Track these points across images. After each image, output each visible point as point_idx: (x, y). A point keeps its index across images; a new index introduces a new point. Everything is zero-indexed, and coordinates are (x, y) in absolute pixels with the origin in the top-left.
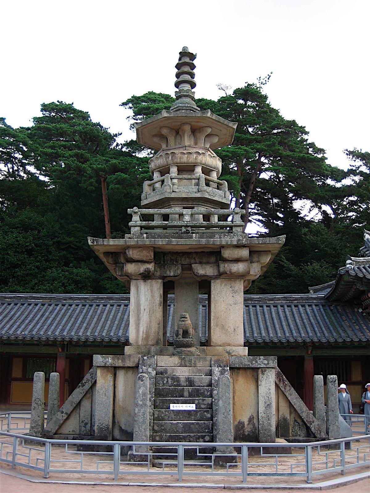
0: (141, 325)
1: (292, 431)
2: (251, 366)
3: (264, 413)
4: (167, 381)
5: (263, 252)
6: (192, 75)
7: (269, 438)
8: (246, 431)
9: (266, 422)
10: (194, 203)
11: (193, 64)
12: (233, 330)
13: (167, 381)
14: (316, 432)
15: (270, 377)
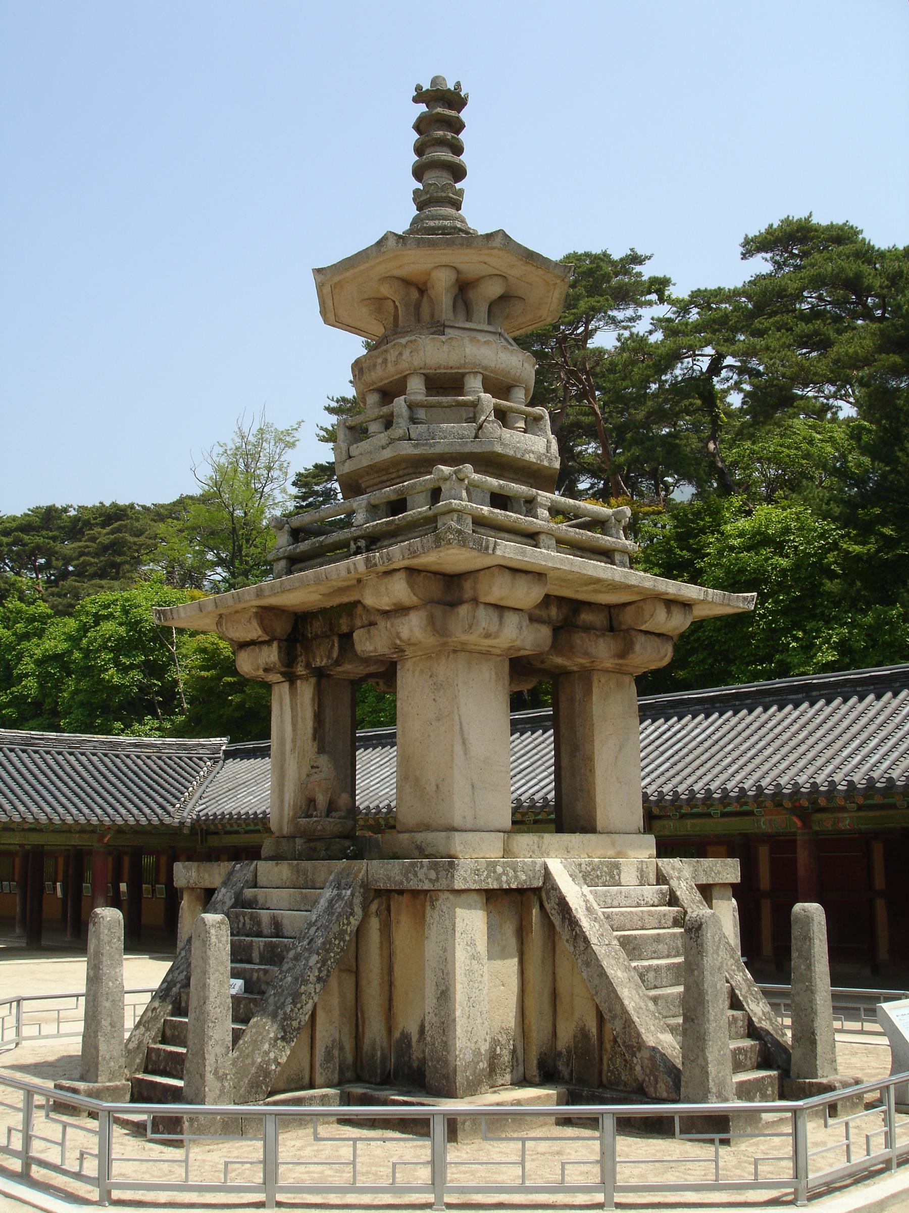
0: (286, 788)
1: (609, 1071)
2: (406, 885)
3: (436, 1015)
4: (244, 924)
5: (482, 573)
6: (458, 150)
7: (444, 1082)
8: (414, 1057)
9: (439, 1040)
10: (401, 473)
11: (458, 118)
12: (434, 788)
13: (244, 924)
14: (647, 1079)
15: (447, 916)
